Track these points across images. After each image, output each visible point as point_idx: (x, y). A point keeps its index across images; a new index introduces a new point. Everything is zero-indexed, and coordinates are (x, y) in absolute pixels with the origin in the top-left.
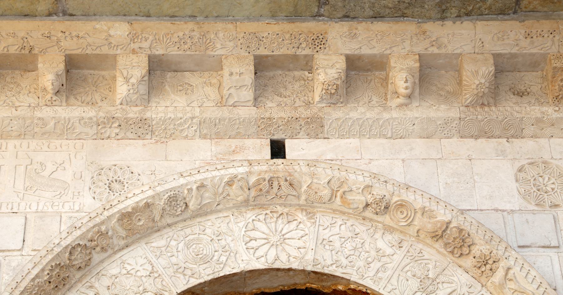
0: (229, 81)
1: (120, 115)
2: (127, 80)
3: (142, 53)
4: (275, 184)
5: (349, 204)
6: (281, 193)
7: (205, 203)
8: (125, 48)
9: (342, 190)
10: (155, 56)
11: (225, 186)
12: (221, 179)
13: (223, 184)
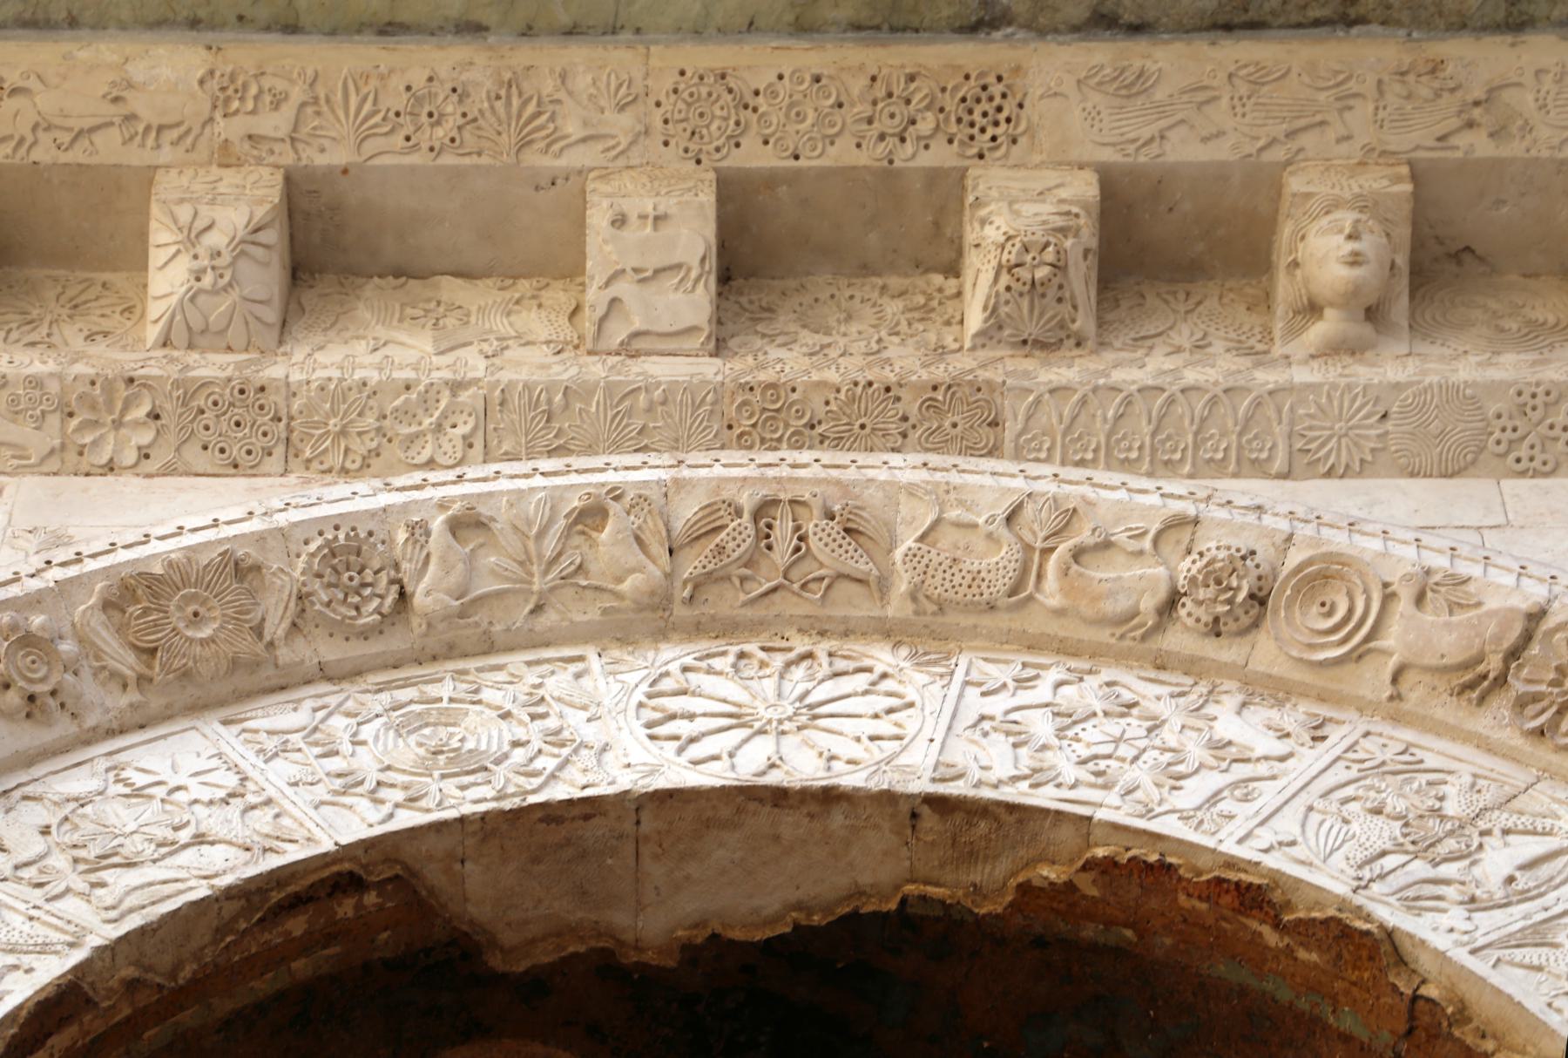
0: (608, 248)
1: (155, 372)
2: (192, 237)
3: (259, 161)
4: (783, 531)
5: (1096, 599)
6: (807, 569)
7: (479, 592)
8: (189, 140)
9: (1063, 548)
10: (310, 173)
11: (569, 527)
12: (554, 499)
13: (561, 523)
